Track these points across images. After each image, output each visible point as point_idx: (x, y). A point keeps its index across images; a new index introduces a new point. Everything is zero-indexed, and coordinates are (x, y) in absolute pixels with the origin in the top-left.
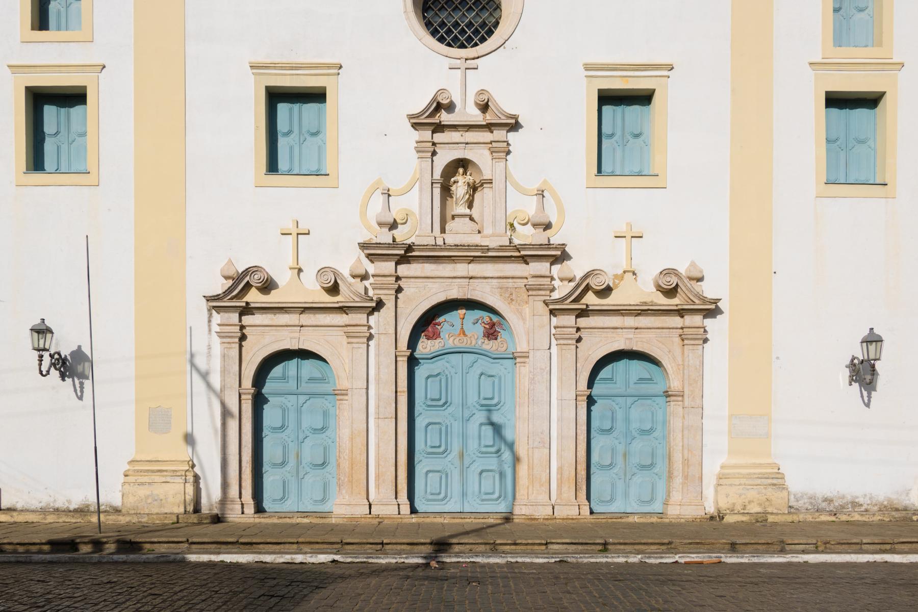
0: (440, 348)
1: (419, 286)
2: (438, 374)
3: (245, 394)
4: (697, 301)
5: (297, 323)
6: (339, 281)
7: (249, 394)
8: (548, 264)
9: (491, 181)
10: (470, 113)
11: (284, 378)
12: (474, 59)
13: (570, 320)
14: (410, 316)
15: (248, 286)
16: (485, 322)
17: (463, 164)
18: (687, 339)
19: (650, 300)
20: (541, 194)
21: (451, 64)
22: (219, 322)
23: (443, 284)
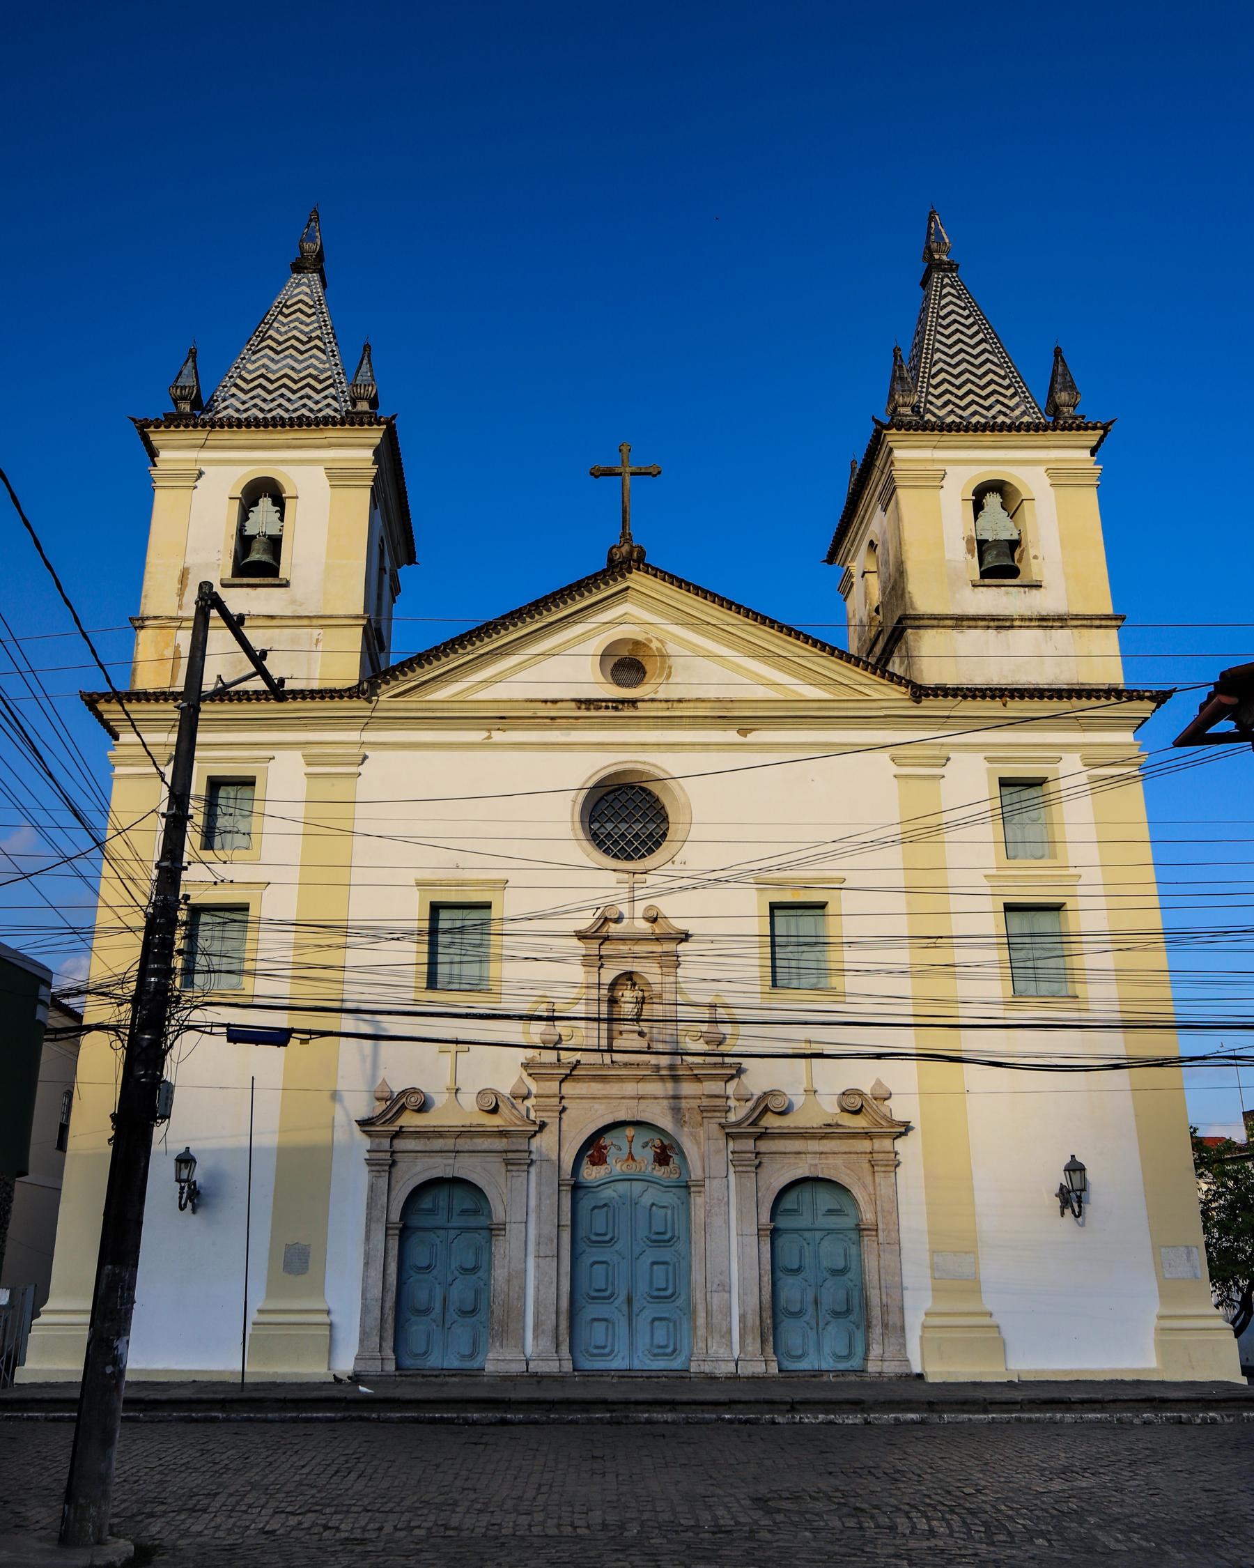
0: (607, 1176)
2: (605, 1205)
3: (392, 1229)
4: (884, 1123)
5: (452, 1148)
6: (500, 1103)
7: (396, 1228)
8: (723, 1084)
12: (641, 873)
13: (748, 1144)
15: (403, 1108)
17: (629, 976)
18: (877, 1165)
22: (369, 1148)
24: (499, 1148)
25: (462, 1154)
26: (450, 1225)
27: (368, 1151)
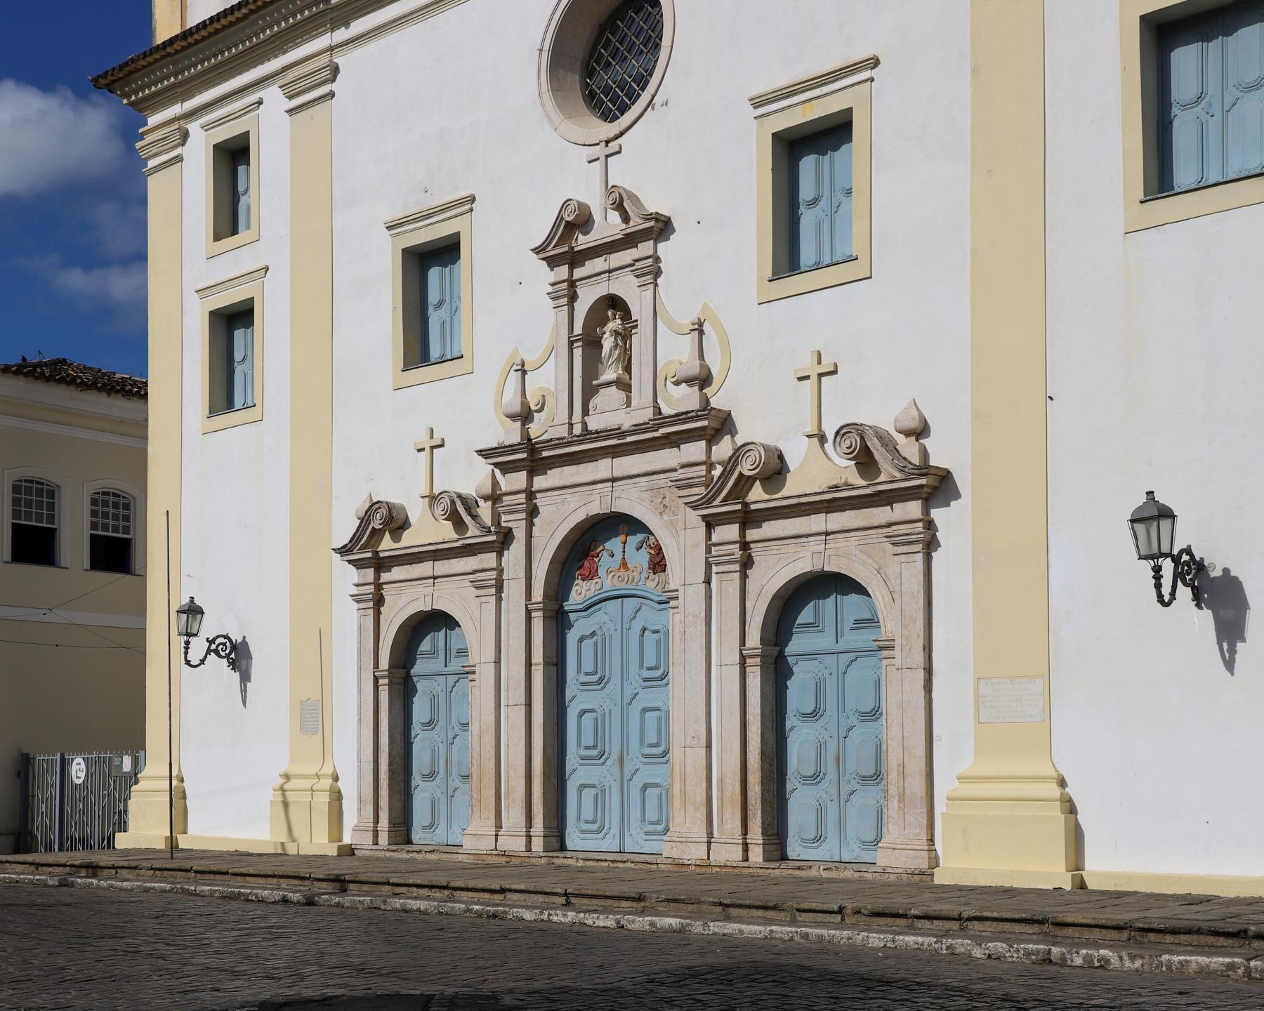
1: (557, 501)
2: (593, 634)
9: (635, 324)
10: (608, 226)
11: (432, 653)
12: (617, 137)
14: (547, 548)
16: (652, 545)
19: (843, 480)
20: (699, 328)
21: (588, 155)
22: (356, 581)
23: (584, 493)
24: (469, 569)
25: (440, 580)
26: (449, 669)
27: (357, 585)
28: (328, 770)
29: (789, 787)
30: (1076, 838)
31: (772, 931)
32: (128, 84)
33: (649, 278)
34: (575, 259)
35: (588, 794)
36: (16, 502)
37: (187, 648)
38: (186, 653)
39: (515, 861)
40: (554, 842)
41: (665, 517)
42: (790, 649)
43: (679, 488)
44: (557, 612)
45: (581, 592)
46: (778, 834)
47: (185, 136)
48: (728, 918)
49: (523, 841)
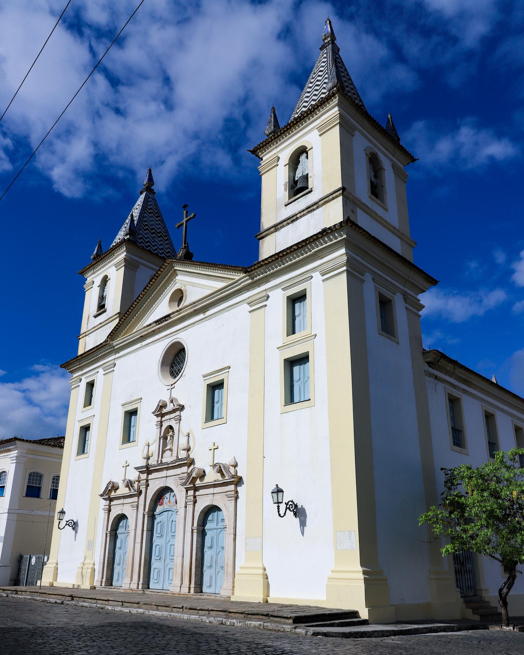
2: (161, 522)
10: (170, 407)
20: (188, 435)
22: (105, 505)
28: (92, 562)
29: (204, 570)
30: (267, 587)
31: (163, 614)
32: (69, 367)
33: (178, 421)
34: (162, 415)
35: (156, 570)
36: (29, 479)
37: (59, 524)
38: (59, 525)
39: (134, 592)
40: (146, 586)
41: (178, 488)
42: (206, 528)
43: (181, 480)
44: (153, 515)
45: (159, 509)
46: (200, 584)
47: (81, 380)
48: (157, 610)
49: (136, 585)
